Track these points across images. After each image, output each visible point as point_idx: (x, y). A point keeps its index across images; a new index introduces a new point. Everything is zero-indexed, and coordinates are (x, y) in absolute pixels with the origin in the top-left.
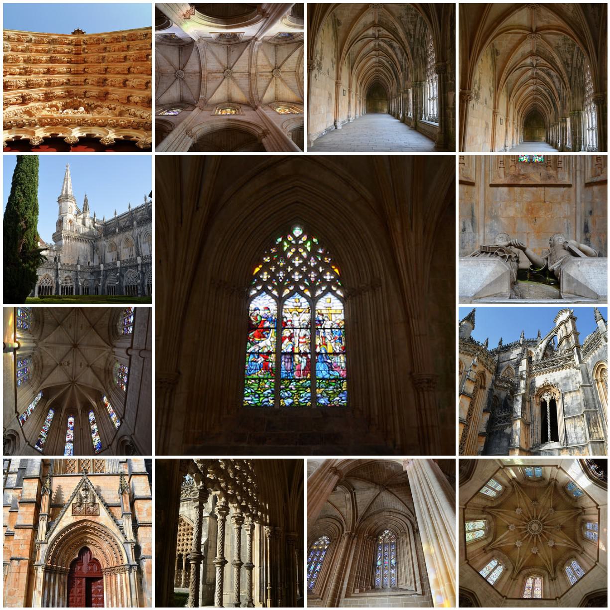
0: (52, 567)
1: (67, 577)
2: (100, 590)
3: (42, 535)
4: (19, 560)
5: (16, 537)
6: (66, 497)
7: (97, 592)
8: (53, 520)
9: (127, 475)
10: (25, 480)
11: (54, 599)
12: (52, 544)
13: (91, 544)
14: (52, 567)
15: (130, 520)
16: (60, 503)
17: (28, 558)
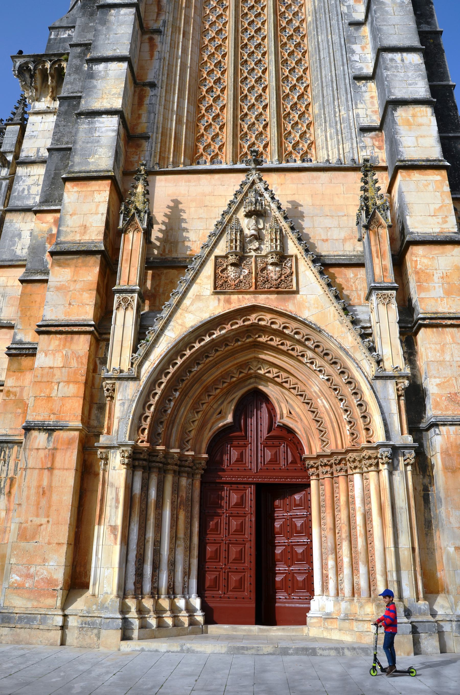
0: (152, 452)
1: (197, 484)
2: (299, 523)
3: (120, 354)
4: (50, 430)
5: (41, 360)
6: (196, 236)
7: (290, 529)
8: (156, 309)
9: (384, 169)
10: (68, 185)
11: (157, 552)
12: (154, 381)
13: (273, 381)
14: (152, 452)
15: (394, 307)
16: (179, 255)
17: (78, 424)
